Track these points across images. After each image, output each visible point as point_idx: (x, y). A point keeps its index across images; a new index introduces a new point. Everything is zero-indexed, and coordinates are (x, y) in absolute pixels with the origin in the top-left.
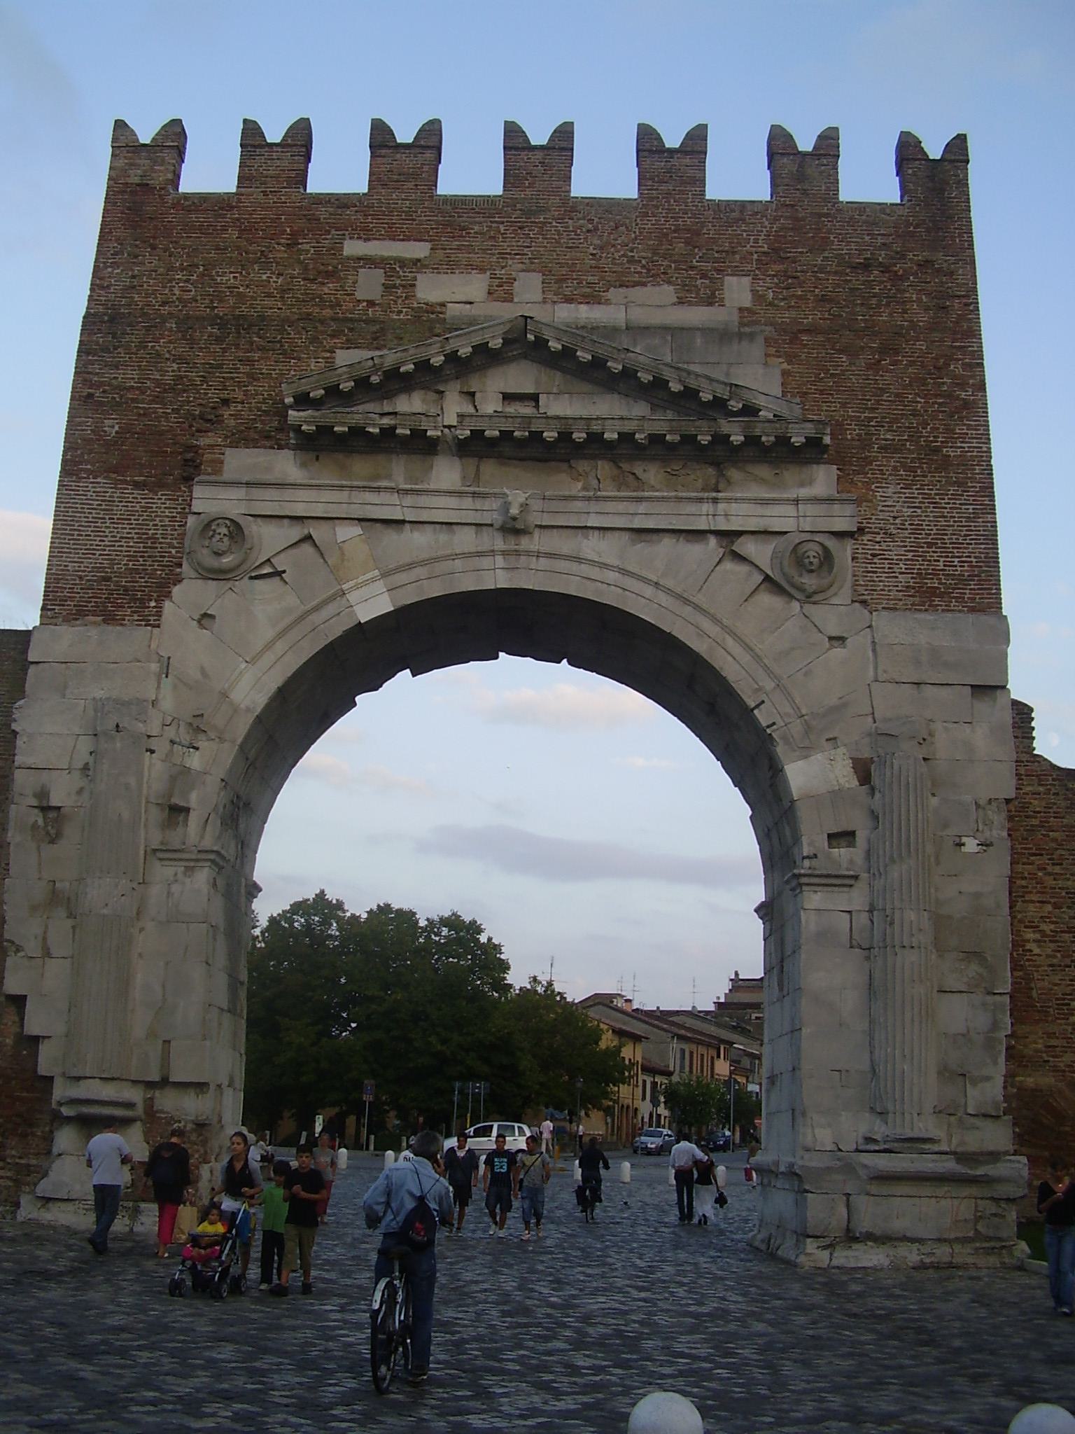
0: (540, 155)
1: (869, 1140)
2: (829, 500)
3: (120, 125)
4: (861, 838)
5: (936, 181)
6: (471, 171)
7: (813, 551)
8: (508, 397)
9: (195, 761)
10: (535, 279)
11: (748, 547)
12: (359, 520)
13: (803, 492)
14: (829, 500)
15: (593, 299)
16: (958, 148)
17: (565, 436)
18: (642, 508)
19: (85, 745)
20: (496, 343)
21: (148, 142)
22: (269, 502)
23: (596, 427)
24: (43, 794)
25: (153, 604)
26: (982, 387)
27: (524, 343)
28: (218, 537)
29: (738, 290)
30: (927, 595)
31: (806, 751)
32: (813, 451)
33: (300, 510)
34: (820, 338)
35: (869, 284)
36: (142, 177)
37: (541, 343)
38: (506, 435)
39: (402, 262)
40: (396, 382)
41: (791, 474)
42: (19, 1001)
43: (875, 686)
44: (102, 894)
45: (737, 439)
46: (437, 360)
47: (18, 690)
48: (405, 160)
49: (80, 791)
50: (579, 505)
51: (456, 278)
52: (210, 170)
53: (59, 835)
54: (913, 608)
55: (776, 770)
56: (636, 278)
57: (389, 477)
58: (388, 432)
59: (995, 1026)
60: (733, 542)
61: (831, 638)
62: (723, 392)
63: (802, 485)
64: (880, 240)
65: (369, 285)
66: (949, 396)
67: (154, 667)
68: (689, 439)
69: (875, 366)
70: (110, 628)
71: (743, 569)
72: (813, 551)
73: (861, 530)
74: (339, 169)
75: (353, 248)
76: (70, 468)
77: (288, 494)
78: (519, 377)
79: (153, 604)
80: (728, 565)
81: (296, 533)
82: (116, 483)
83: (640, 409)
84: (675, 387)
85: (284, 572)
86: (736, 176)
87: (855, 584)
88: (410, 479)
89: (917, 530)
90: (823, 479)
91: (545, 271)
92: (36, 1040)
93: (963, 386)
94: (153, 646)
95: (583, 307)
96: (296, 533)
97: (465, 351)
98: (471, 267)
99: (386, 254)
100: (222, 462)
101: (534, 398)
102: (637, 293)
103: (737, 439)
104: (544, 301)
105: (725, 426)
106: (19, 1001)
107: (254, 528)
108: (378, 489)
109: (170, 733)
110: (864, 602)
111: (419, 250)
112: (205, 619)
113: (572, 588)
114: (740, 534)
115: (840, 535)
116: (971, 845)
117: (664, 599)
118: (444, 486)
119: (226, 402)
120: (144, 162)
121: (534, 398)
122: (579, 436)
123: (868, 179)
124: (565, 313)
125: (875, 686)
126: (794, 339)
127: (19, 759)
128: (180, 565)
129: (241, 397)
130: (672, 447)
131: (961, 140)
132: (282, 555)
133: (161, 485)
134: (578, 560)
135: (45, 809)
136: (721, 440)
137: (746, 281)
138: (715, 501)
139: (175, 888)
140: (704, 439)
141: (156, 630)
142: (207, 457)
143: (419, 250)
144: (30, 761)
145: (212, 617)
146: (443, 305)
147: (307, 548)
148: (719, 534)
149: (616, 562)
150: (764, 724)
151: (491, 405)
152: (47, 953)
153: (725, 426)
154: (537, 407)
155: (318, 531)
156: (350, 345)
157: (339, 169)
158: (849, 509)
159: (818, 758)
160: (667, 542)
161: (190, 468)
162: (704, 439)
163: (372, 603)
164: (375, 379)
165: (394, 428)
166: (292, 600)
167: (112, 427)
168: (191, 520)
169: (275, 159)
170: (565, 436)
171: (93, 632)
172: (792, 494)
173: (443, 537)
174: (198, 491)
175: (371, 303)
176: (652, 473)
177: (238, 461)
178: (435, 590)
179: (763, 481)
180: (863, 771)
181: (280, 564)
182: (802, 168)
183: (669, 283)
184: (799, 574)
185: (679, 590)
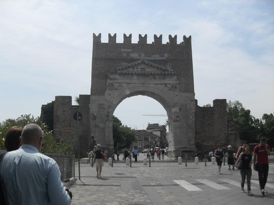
1: (181, 147)
2: (176, 80)
3: (94, 34)
5: (188, 41)
7: (174, 86)
8: (141, 68)
9: (110, 110)
10: (143, 54)
11: (168, 85)
14: (176, 80)
15: (150, 57)
16: (190, 37)
19: (98, 109)
27: (143, 63)
29: (166, 55)
31: (174, 108)
33: (119, 82)
36: (97, 39)
38: (142, 73)
39: (129, 52)
40: (129, 67)
42: (93, 137)
44: (101, 125)
45: (166, 74)
47: (89, 103)
48: (128, 39)
49: (97, 114)
52: (105, 40)
53: (95, 119)
55: (170, 109)
58: (129, 73)
62: (165, 68)
63: (173, 78)
65: (125, 55)
67: (104, 100)
68: (161, 74)
71: (167, 88)
72: (174, 86)
74: (120, 40)
75: (123, 50)
78: (143, 66)
81: (119, 84)
83: (156, 70)
84: (160, 68)
90: (175, 77)
92: (95, 141)
95: (149, 58)
96: (119, 84)
101: (144, 68)
103: (166, 74)
105: (165, 72)
111: (130, 50)
114: (167, 84)
115: (177, 84)
116: (191, 117)
119: (110, 69)
121: (144, 68)
122: (150, 74)
130: (159, 75)
131: (190, 36)
134: (149, 87)
135: (94, 116)
137: (167, 54)
138: (164, 80)
140: (163, 74)
143: (130, 50)
145: (110, 94)
147: (120, 86)
148: (164, 84)
151: (139, 70)
152: (96, 132)
153: (165, 72)
158: (178, 81)
159: (175, 108)
160: (159, 85)
161: (107, 77)
163: (128, 92)
164: (127, 67)
169: (112, 38)
173: (135, 85)
175: (125, 57)
176: (157, 77)
177: (112, 76)
180: (180, 109)
181: (117, 88)
182: (173, 39)
183: (158, 54)
184: (173, 88)
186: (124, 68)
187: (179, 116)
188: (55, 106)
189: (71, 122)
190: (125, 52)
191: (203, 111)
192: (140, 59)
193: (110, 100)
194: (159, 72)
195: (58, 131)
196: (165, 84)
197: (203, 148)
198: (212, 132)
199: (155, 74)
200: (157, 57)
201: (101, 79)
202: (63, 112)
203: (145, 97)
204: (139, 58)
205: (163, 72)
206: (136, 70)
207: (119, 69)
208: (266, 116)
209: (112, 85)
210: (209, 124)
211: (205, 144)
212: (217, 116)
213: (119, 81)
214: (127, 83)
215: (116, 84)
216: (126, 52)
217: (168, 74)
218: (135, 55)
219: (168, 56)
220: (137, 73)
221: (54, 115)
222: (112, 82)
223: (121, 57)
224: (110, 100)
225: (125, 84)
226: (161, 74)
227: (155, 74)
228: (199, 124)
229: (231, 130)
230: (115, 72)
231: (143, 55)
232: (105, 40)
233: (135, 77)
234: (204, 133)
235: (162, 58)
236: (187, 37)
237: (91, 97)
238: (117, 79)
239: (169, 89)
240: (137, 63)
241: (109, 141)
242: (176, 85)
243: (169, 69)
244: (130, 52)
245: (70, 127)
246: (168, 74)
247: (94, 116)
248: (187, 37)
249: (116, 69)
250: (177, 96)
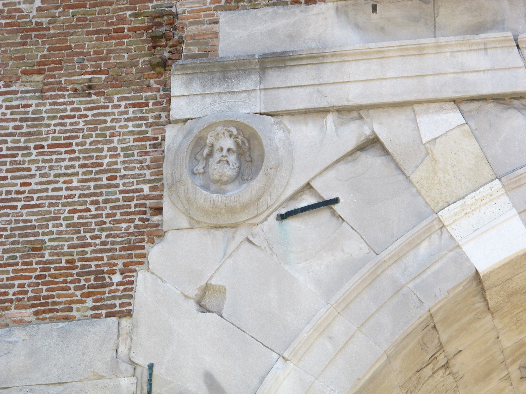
12: (456, 102)
25: (117, 278)
28: (217, 156)
33: (353, 95)
70: (47, 326)
77: (328, 72)
79: (117, 278)
82: (41, 93)
85: (336, 201)
94: (123, 349)
96: (352, 133)
100: (216, 35)
107: (278, 135)
128: (159, 210)
132: (331, 174)
133: (117, 82)
141: (125, 322)
142: (191, 30)
145: (221, 291)
147: (370, 159)
166: (355, 247)
168: (171, 133)
171: (19, 335)
174: (178, 85)
209: (249, 153)
213: (355, 83)
214: (456, 102)
215: (305, 132)
222: (246, 101)
238: (316, 58)
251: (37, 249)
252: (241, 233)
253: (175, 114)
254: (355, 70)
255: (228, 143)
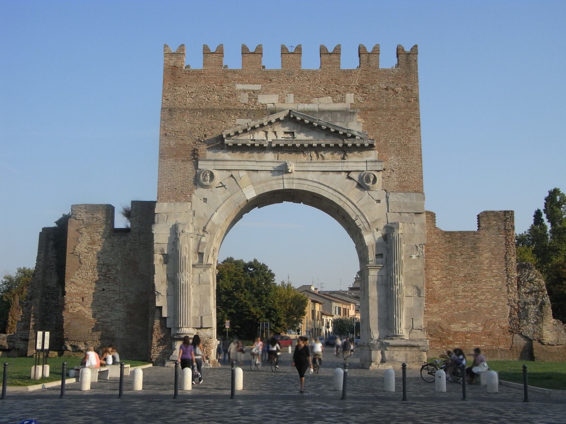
0: (292, 56)
2: (376, 161)
3: (166, 46)
4: (384, 256)
5: (407, 58)
6: (272, 61)
8: (285, 133)
9: (203, 240)
10: (292, 95)
11: (353, 175)
13: (369, 159)
15: (309, 102)
17: (302, 145)
18: (324, 165)
20: (282, 118)
21: (175, 52)
22: (220, 165)
23: (311, 143)
24: (162, 250)
26: (419, 125)
29: (350, 98)
30: (403, 188)
32: (371, 147)
34: (373, 112)
35: (388, 95)
37: (294, 118)
39: (254, 92)
41: (365, 153)
42: (160, 308)
43: (388, 213)
45: (350, 145)
46: (265, 123)
50: (307, 164)
51: (269, 96)
54: (399, 191)
55: (361, 237)
56: (321, 95)
57: (253, 157)
58: (253, 145)
59: (421, 305)
60: (349, 174)
61: (376, 200)
62: (345, 131)
63: (368, 157)
64: (391, 81)
65: (244, 98)
66: (410, 128)
67: (191, 213)
68: (336, 145)
69: (389, 120)
71: (352, 181)
73: (384, 169)
74: (233, 61)
76: (162, 156)
77: (225, 163)
80: (348, 180)
81: (229, 174)
82: (176, 160)
83: (323, 135)
84: (332, 130)
86: (349, 61)
87: (383, 185)
88: (260, 158)
89: (400, 168)
90: (373, 155)
91: (294, 93)
92: (165, 318)
93: (413, 125)
95: (306, 104)
96: (229, 174)
97: (273, 121)
98: (272, 94)
99: (249, 88)
101: (292, 133)
102: (321, 100)
103: (350, 145)
104: (295, 103)
105: (346, 142)
106: (160, 308)
108: (251, 161)
109: (197, 232)
110: (385, 190)
111: (257, 87)
112: (205, 200)
113: (305, 188)
116: (414, 257)
117: (330, 191)
118: (269, 159)
120: (174, 59)
122: (306, 145)
123: (388, 61)
124: (301, 107)
125: (388, 213)
126: (366, 113)
127: (155, 241)
129: (210, 134)
130: (332, 147)
131: (416, 46)
133: (188, 160)
134: (306, 180)
136: (345, 145)
139: (201, 275)
140: (341, 145)
143: (257, 87)
144: (159, 241)
146: (266, 104)
149: (317, 181)
150: (358, 225)
153: (346, 142)
154: (294, 135)
155: (235, 174)
156: (240, 117)
157: (233, 61)
160: (331, 174)
162: (341, 145)
163: (251, 194)
164: (249, 129)
165: (254, 144)
167: (172, 143)
170: (302, 145)
171: (172, 204)
172: (365, 159)
174: (200, 163)
175: (245, 104)
178: (267, 190)
179: (357, 156)
185: (334, 188)
186: (240, 132)
187: (382, 255)
188: (71, 229)
189: (109, 271)
190: (245, 91)
191: (449, 242)
192: (281, 110)
193: (205, 215)
194: (331, 142)
195: (76, 294)
196: (349, 172)
197: (451, 339)
198: (475, 297)
199: (319, 145)
200: (326, 103)
201: (183, 161)
202: (89, 244)
203: (301, 206)
204: (279, 106)
205: (341, 141)
206: (271, 137)
207: (229, 136)
208: (57, 223)
209: (212, 176)
210: (465, 277)
211: (455, 327)
212: (488, 255)
215: (221, 172)
216: (248, 90)
217: (354, 145)
218: (269, 100)
219: (354, 100)
220: (274, 145)
221: (69, 250)
223: (236, 104)
224: (205, 215)
225: (243, 174)
226: (336, 145)
227: (319, 145)
228: (439, 277)
229: (525, 293)
230: (219, 144)
231: (291, 98)
232: (194, 60)
233: (270, 156)
234: (453, 298)
235: (339, 106)
236: (407, 49)
237: (157, 205)
239: (356, 184)
240: (273, 119)
241: (202, 317)
242: (375, 173)
243: (356, 134)
244: (259, 92)
245: (108, 282)
246: (354, 145)
247: (163, 255)
248: (407, 49)
249: (222, 135)
250: (379, 201)
251: (176, 189)
252: (210, 189)
253: (199, 168)
254: (229, 163)
255: (208, 174)
